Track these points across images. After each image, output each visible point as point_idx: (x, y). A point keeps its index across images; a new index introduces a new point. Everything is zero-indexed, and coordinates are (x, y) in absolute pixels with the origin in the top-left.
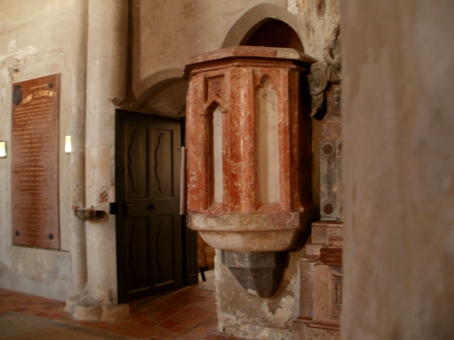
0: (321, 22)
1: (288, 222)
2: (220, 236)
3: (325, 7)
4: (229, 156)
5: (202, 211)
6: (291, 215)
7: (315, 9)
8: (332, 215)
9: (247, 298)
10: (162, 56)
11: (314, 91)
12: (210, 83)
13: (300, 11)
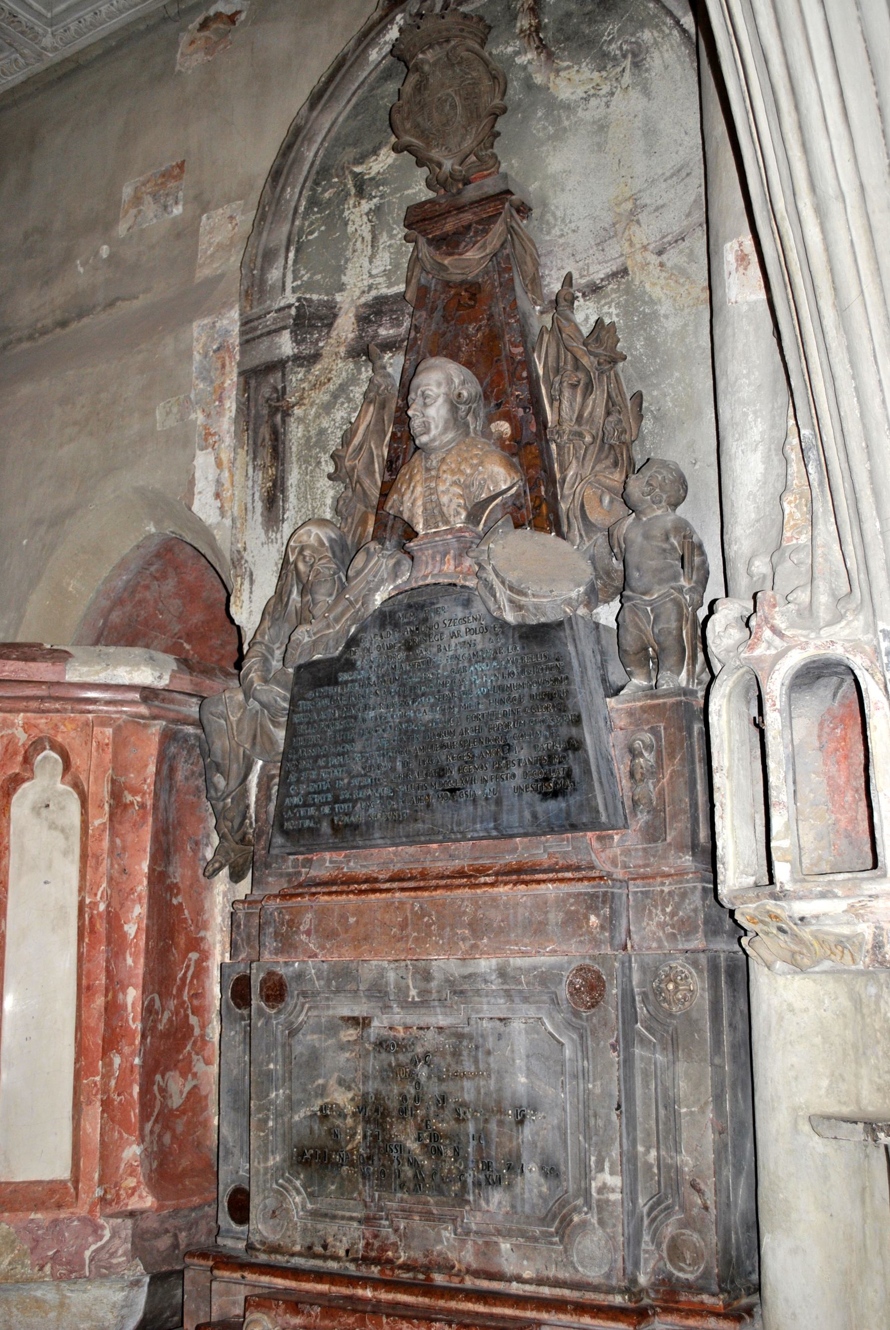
1: (87, 1254)
6: (102, 1227)
7: (259, 506)
13: (223, 513)
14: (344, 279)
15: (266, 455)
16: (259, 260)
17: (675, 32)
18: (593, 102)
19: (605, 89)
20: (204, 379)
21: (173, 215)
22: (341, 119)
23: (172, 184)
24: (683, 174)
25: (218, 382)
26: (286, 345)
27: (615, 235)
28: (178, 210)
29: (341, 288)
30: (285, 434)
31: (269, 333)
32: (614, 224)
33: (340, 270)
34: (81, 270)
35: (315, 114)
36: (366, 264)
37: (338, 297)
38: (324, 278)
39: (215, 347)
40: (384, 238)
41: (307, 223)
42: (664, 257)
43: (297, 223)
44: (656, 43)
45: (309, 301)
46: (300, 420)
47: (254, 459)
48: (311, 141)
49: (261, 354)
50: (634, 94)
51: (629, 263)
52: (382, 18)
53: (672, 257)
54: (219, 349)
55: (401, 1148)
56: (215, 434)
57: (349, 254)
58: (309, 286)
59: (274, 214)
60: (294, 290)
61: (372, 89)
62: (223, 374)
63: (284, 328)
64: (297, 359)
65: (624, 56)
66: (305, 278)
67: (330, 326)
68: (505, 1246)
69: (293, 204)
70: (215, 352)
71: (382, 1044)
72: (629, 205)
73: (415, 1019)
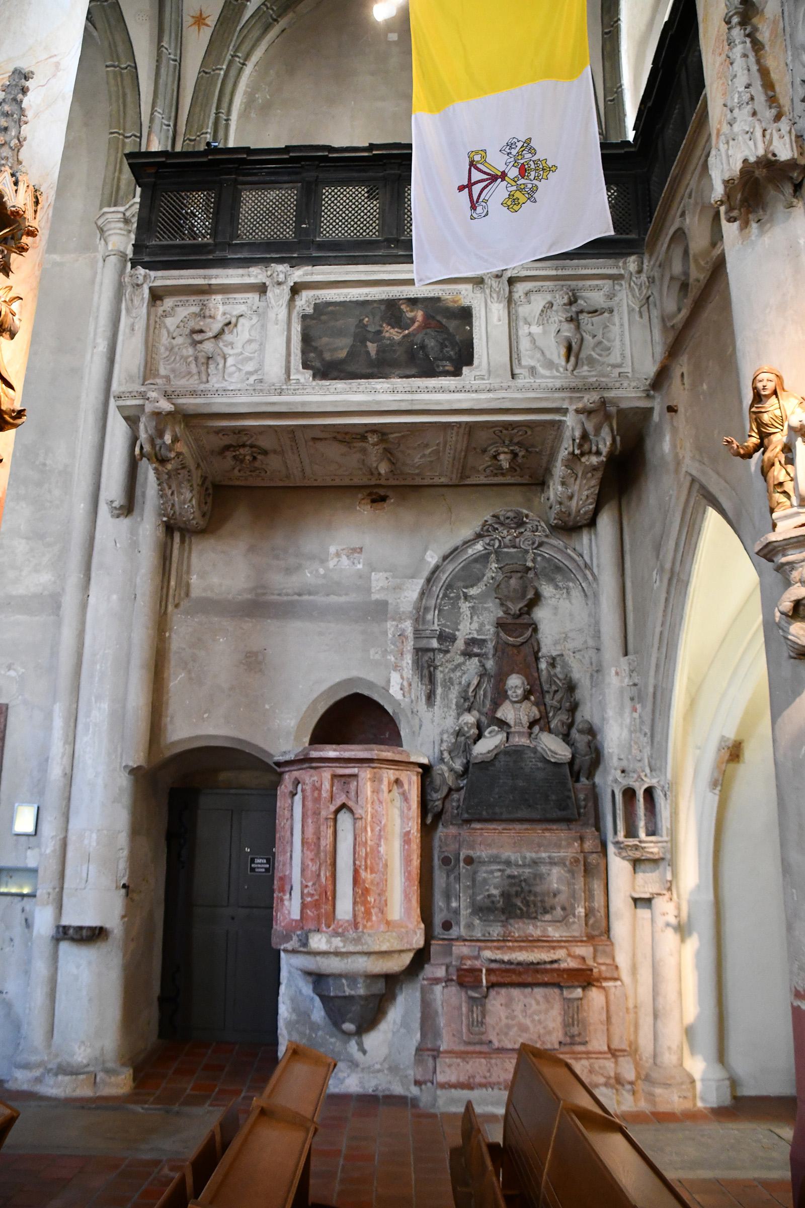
0: (430, 714)
2: (338, 959)
3: (435, 698)
4: (363, 867)
5: (324, 929)
7: (424, 698)
8: (451, 931)
9: (328, 1037)
10: (206, 715)
11: (432, 797)
12: (336, 781)
13: (404, 696)
14: (459, 627)
15: (426, 680)
16: (422, 610)
18: (553, 599)
19: (557, 596)
20: (393, 645)
23: (356, 555)
25: (402, 647)
26: (435, 644)
28: (360, 566)
29: (458, 630)
30: (434, 675)
34: (309, 575)
35: (445, 563)
36: (468, 624)
37: (457, 633)
40: (475, 618)
43: (439, 601)
46: (441, 672)
47: (421, 680)
48: (444, 572)
49: (423, 644)
50: (567, 601)
51: (564, 653)
52: (473, 540)
53: (578, 656)
54: (400, 635)
55: (516, 905)
57: (461, 618)
58: (445, 625)
60: (438, 625)
61: (469, 563)
64: (440, 650)
67: (454, 642)
68: (550, 929)
71: (510, 877)
72: (564, 635)
73: (521, 870)
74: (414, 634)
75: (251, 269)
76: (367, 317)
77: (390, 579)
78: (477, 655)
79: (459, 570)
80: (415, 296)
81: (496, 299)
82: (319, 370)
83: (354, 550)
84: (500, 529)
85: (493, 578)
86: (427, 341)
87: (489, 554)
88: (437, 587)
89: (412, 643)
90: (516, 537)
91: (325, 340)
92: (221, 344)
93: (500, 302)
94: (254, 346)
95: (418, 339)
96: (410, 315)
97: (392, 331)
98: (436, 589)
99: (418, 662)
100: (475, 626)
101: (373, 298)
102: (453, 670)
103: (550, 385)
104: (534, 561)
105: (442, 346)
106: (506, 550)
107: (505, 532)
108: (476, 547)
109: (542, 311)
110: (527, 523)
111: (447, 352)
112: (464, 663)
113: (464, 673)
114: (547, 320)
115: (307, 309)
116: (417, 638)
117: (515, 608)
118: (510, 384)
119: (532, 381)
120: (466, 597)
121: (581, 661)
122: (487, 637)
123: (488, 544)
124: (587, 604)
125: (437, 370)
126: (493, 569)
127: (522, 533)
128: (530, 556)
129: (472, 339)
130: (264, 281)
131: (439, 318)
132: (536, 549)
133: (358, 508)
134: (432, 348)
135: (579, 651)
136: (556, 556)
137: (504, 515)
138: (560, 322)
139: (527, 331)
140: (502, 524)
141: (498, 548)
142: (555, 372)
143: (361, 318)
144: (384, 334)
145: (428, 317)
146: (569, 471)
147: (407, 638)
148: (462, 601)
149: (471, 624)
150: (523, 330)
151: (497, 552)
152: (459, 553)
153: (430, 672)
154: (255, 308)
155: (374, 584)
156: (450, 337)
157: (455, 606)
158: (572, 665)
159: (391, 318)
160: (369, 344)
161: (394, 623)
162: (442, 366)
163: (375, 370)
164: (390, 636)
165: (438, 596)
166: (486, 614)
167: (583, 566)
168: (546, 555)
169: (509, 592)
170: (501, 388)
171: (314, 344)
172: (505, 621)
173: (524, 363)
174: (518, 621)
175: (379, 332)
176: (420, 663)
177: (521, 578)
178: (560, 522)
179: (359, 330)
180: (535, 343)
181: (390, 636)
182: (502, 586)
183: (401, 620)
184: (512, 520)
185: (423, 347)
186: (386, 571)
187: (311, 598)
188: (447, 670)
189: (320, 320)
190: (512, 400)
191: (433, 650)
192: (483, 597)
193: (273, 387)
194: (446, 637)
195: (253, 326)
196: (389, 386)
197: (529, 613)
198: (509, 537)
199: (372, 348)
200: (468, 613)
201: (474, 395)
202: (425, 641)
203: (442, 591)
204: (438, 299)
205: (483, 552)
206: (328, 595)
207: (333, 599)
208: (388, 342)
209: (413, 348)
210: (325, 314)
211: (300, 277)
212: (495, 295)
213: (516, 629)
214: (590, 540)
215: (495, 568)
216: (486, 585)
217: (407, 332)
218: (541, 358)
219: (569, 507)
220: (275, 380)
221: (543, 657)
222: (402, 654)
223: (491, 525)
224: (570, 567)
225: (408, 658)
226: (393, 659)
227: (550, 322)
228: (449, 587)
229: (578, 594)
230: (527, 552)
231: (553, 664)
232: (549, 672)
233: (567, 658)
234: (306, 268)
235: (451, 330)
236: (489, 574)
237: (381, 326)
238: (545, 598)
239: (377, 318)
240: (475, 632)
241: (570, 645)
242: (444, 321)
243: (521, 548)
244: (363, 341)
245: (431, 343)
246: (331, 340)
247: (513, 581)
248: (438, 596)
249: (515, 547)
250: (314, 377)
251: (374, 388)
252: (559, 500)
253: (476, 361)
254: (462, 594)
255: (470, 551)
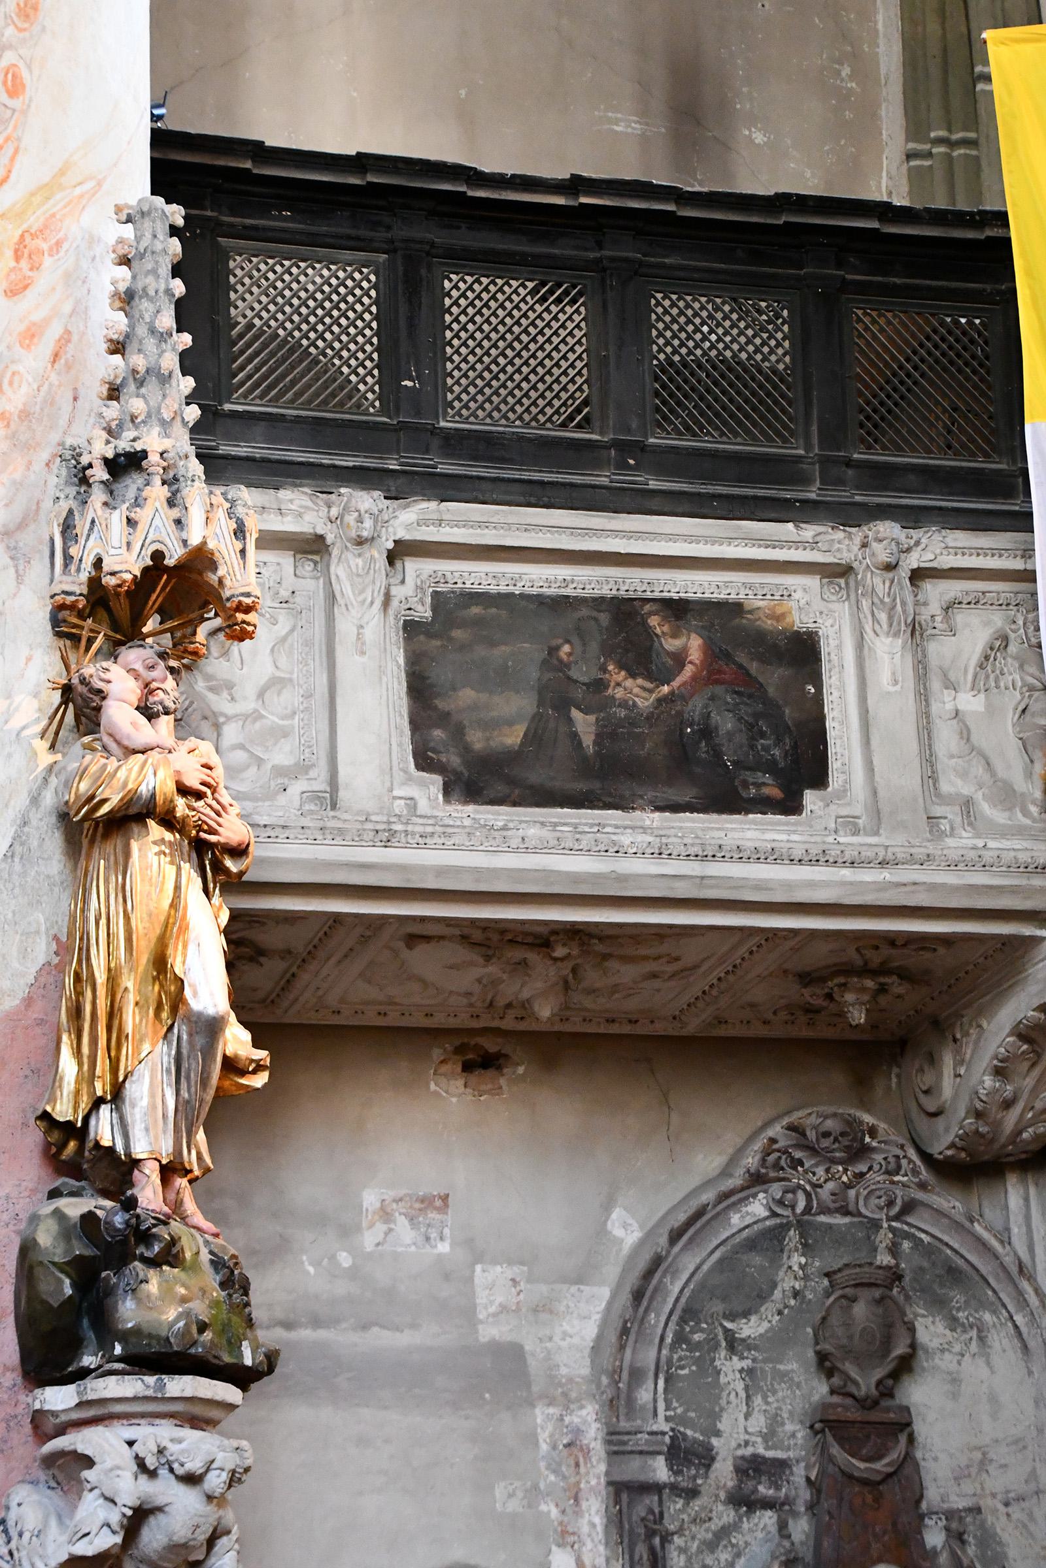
14: (719, 1425)
16: (625, 1375)
17: (1010, 1324)
18: (947, 1356)
19: (957, 1348)
20: (554, 1472)
21: (435, 1251)
22: (705, 1267)
23: (433, 1215)
24: (1021, 1445)
25: (573, 1480)
26: (660, 1470)
27: (969, 1476)
28: (444, 1248)
29: (718, 1434)
30: (664, 1558)
31: (641, 1452)
32: (968, 1467)
33: (715, 1416)
34: (311, 1270)
35: (676, 1249)
36: (741, 1417)
37: (715, 1441)
38: (699, 1417)
39: (565, 1442)
40: (758, 1400)
41: (675, 1357)
42: (1010, 1510)
43: (665, 1352)
44: (994, 1325)
45: (684, 1435)
46: (682, 1550)
48: (675, 1274)
49: (632, 1470)
50: (981, 1362)
51: (982, 1503)
52: (743, 1189)
53: (1016, 1511)
56: (574, 1534)
57: (723, 1402)
58: (682, 1420)
59: (639, 1333)
60: (667, 1419)
61: (736, 1251)
62: (578, 1473)
63: (659, 1453)
64: (674, 1487)
65: (971, 1327)
66: (679, 1411)
67: (708, 1467)
69: (659, 1331)
70: (565, 1446)
72: (978, 1455)
74: (608, 1442)
75: (285, 494)
76: (568, 641)
77: (522, 1285)
78: (768, 1504)
79: (712, 1270)
80: (682, 595)
81: (885, 626)
82: (458, 775)
83: (427, 1202)
84: (807, 1165)
85: (796, 1294)
86: (715, 718)
87: (784, 1228)
88: (658, 1316)
89: (603, 1468)
90: (848, 1186)
91: (467, 695)
92: (200, 685)
93: (896, 635)
94: (289, 698)
95: (696, 706)
96: (671, 645)
97: (629, 683)
98: (656, 1320)
99: (621, 1522)
100: (758, 1422)
101: (579, 592)
102: (711, 1546)
103: (1023, 857)
104: (894, 1250)
105: (754, 732)
106: (822, 1219)
107: (820, 1171)
108: (750, 1209)
109: (987, 658)
110: (874, 1149)
111: (766, 749)
112: (735, 1527)
113: (738, 1555)
114: (997, 680)
115: (420, 608)
116: (616, 1453)
117: (866, 1382)
118: (931, 848)
119: (980, 843)
120: (734, 1344)
121: (1025, 1526)
122: (791, 1454)
123: (780, 1202)
124: (1030, 1373)
125: (744, 795)
126: (796, 1268)
127: (862, 1175)
128: (884, 1238)
129: (821, 719)
130: (320, 531)
131: (742, 658)
132: (897, 1218)
133: (433, 1086)
134: (730, 735)
135: (1021, 1498)
136: (946, 1238)
137: (815, 1127)
138: (1032, 689)
139: (949, 706)
140: (812, 1150)
141: (803, 1213)
142: (1019, 815)
143: (554, 642)
144: (610, 691)
145: (715, 654)
146: (1025, 1047)
147: (587, 1452)
148: (723, 1353)
149: (747, 1416)
150: (944, 703)
151: (802, 1226)
152: (708, 1222)
153: (652, 1551)
154: (284, 594)
155: (482, 1297)
156: (771, 710)
157: (707, 1369)
158: (1005, 1537)
159: (627, 651)
160: (575, 714)
161: (551, 1410)
162: (755, 784)
163: (596, 785)
164: (544, 1447)
165: (662, 1339)
166: (783, 1391)
167: (1014, 1270)
168: (923, 1236)
169: (851, 1337)
170: (911, 860)
171: (440, 704)
172: (840, 1413)
173: (945, 787)
174: (875, 1416)
175: (599, 685)
176: (627, 1526)
177: (880, 1301)
178: (963, 1155)
179: (550, 675)
180: (968, 740)
181: (544, 1447)
182: (834, 1320)
183: (568, 1403)
184: (836, 1140)
185: (707, 732)
186: (510, 1263)
187: (323, 1334)
188: (695, 1546)
189: (450, 639)
190: (932, 887)
191: (656, 1488)
192: (776, 1342)
193: (369, 826)
194: (686, 1452)
195: (284, 639)
196: (651, 839)
197: (890, 1395)
198: (830, 1185)
199: (584, 724)
200: (740, 1386)
201: (846, 873)
202: (636, 1463)
203: (672, 1326)
204: (735, 609)
205: (768, 1223)
206: (365, 1327)
207: (381, 1339)
208: (623, 713)
209: (682, 732)
210: (463, 624)
211: (408, 527)
212: (883, 617)
213: (868, 1437)
214: (1027, 1199)
215: (802, 1267)
216: (780, 1313)
217: (666, 689)
218: (986, 777)
219: (997, 1125)
220: (370, 805)
221: (932, 1513)
222: (576, 1499)
223: (785, 1152)
224: (984, 1270)
225: (593, 1510)
226: (554, 1512)
227: (1002, 684)
228: (689, 1314)
229: (1005, 1341)
230: (875, 1225)
231: (957, 1537)
232: (953, 1554)
233: (990, 1519)
234: (424, 505)
235: (771, 691)
236: (787, 1283)
237: (604, 669)
238: (926, 1351)
239: (594, 647)
240: (759, 1440)
241: (997, 1482)
242: (754, 667)
243: (860, 1214)
244: (563, 705)
245: (725, 723)
246: (484, 697)
247: (860, 1310)
248: (662, 1339)
249: (847, 1213)
250: (447, 791)
251: (614, 843)
252: (979, 1105)
253: (835, 779)
254: (721, 1337)
255: (736, 1220)
